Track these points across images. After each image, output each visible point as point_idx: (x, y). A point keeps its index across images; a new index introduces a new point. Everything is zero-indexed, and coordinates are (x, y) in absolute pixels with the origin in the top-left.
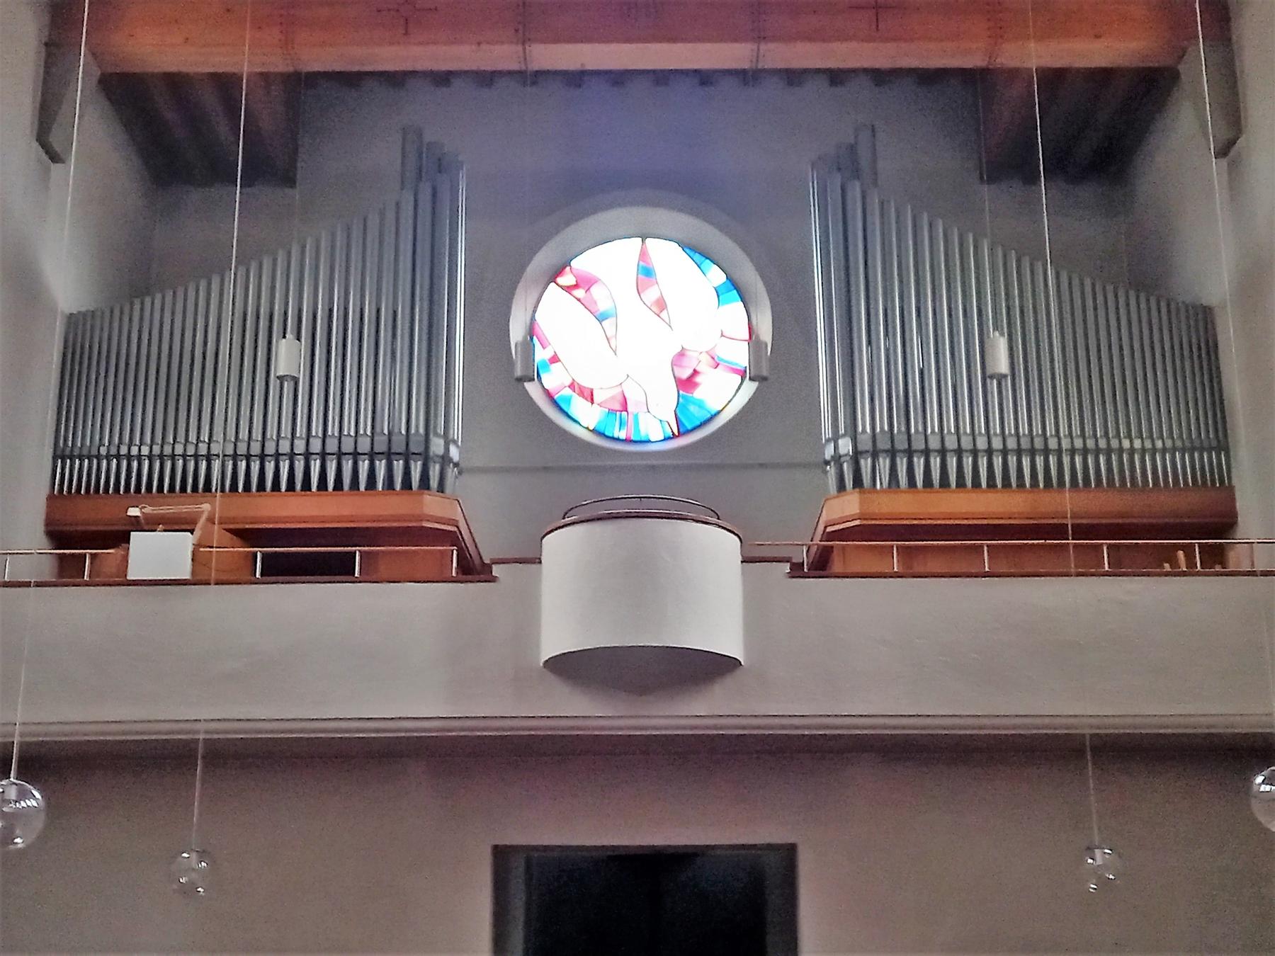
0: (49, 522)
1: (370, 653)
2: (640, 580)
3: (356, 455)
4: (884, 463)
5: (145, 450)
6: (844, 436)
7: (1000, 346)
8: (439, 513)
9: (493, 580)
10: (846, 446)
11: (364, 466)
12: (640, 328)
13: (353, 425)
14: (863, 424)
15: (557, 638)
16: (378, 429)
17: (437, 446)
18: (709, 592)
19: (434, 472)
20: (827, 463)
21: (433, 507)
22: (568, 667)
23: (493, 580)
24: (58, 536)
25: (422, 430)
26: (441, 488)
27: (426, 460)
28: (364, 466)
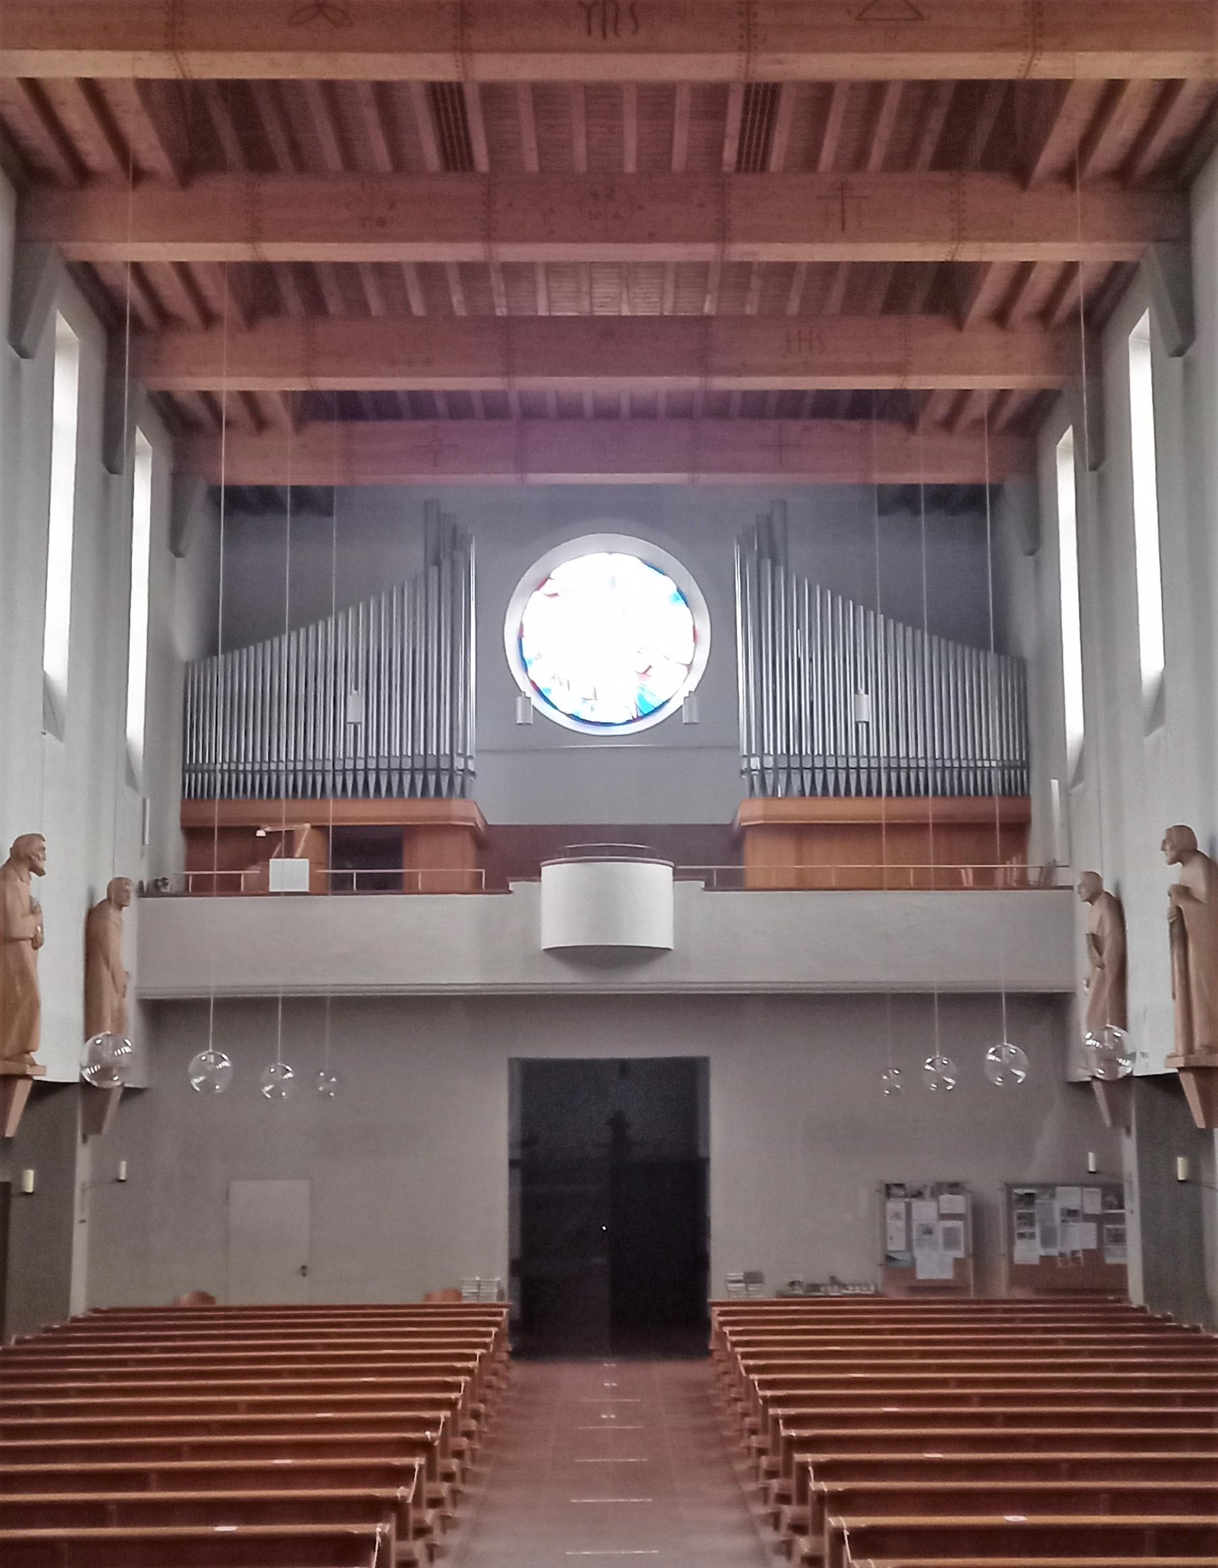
0: (184, 819)
1: (430, 936)
2: (604, 904)
3: (401, 771)
4: (783, 777)
5: (249, 767)
6: (754, 756)
7: (866, 701)
8: (462, 813)
9: (510, 892)
10: (755, 763)
11: (407, 779)
12: (606, 634)
13: (400, 746)
14: (769, 747)
15: (553, 934)
16: (416, 752)
17: (459, 763)
18: (651, 903)
19: (458, 781)
20: (742, 772)
21: (458, 810)
22: (559, 953)
23: (510, 892)
24: (195, 833)
25: (448, 752)
26: (463, 793)
27: (451, 771)
28: (407, 779)
